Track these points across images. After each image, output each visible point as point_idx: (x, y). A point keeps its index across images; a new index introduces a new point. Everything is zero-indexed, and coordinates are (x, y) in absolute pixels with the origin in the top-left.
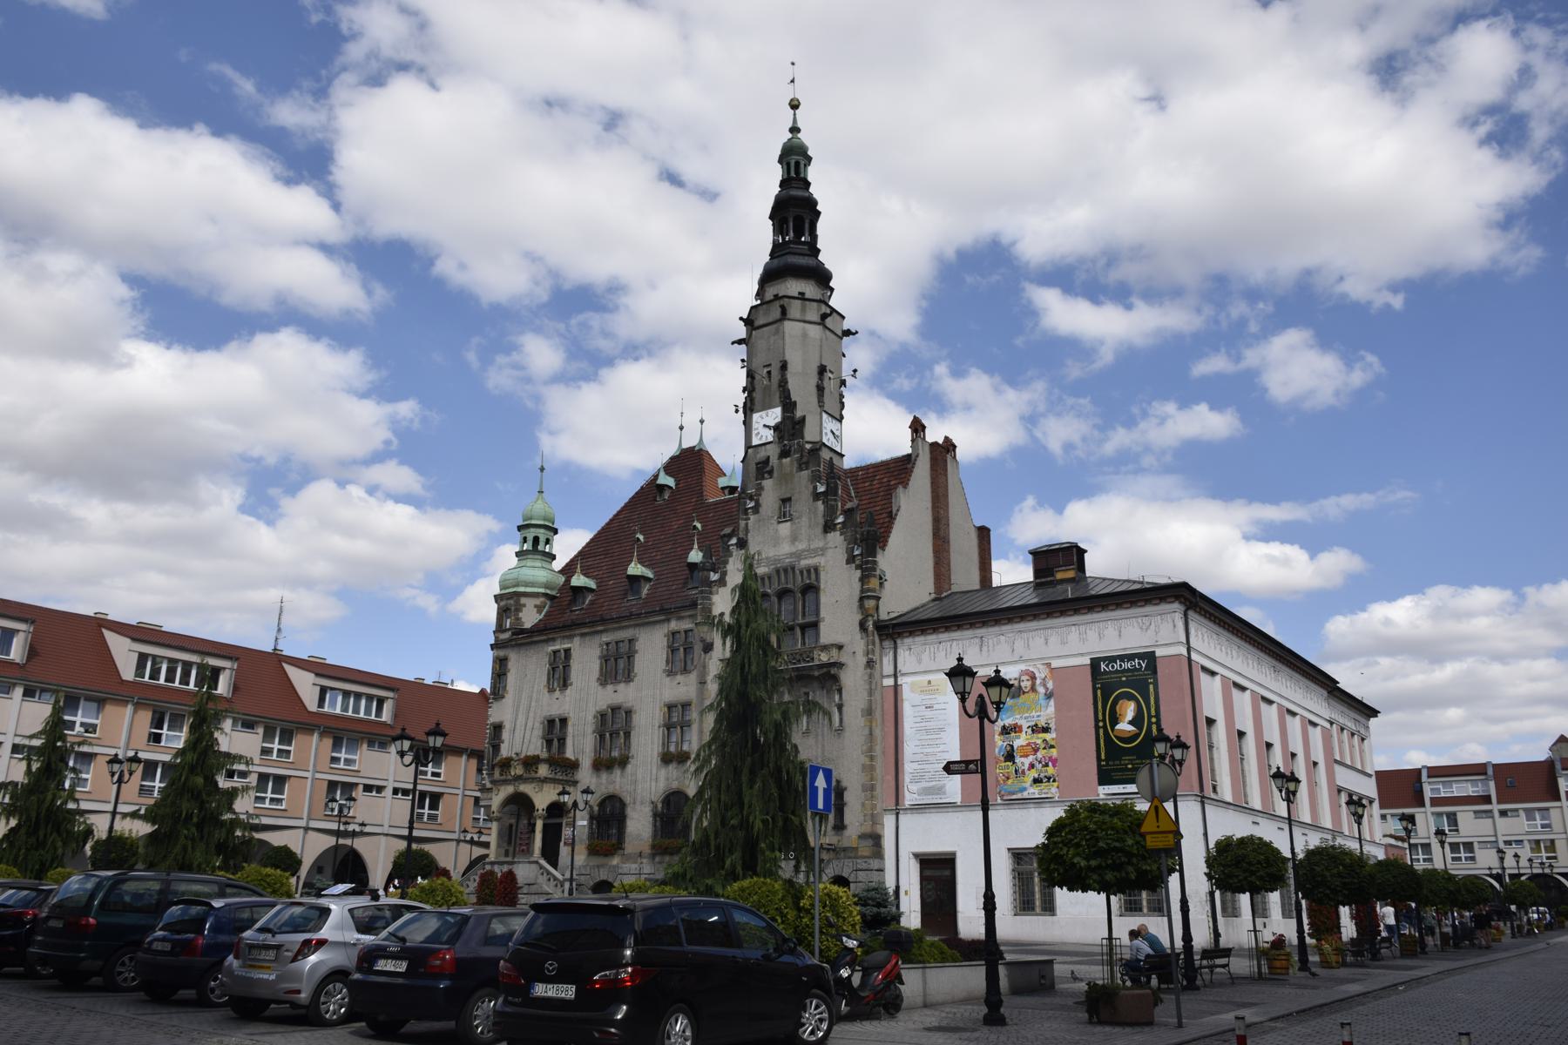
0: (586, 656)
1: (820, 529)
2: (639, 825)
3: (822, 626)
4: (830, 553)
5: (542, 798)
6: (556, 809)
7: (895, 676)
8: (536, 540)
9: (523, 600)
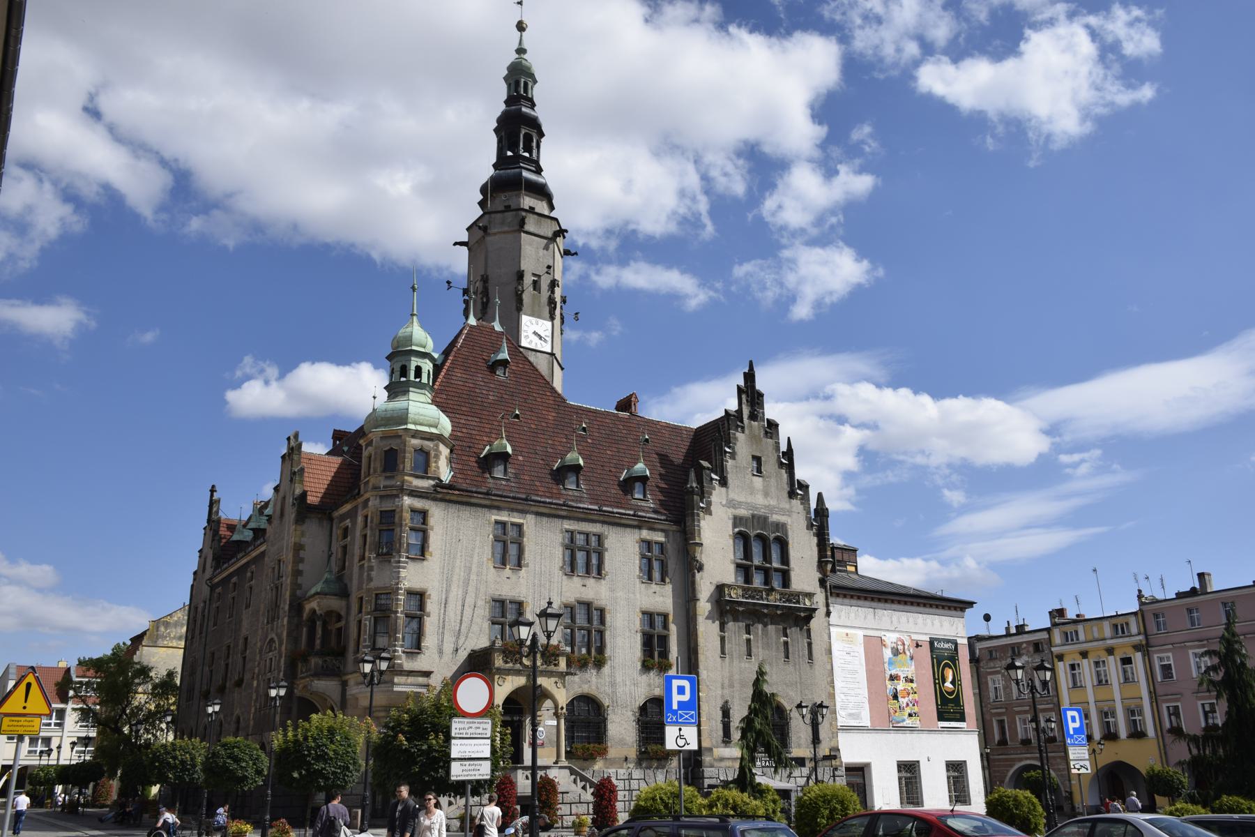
2: (622, 729)
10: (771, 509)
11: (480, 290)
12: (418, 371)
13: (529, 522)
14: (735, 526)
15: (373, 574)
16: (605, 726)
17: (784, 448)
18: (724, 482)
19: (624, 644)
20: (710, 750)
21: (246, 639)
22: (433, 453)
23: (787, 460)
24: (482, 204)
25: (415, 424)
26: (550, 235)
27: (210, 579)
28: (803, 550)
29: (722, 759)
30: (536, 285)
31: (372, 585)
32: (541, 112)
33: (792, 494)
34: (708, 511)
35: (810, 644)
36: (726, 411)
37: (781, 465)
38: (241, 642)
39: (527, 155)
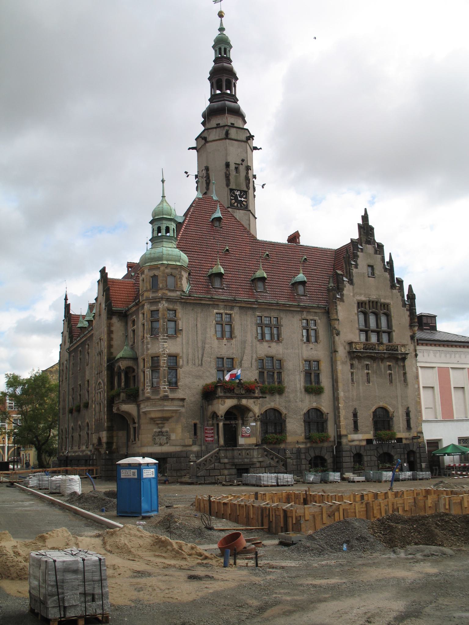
11: (205, 175)
12: (167, 230)
13: (236, 313)
14: (358, 307)
15: (149, 346)
16: (285, 424)
17: (387, 259)
18: (351, 282)
19: (294, 381)
20: (346, 436)
21: (88, 381)
22: (178, 276)
23: (390, 268)
24: (203, 124)
25: (167, 261)
26: (244, 139)
27: (69, 349)
28: (400, 318)
30: (236, 169)
31: (149, 352)
32: (236, 66)
33: (393, 286)
34: (342, 300)
35: (405, 374)
36: (351, 239)
37: (386, 270)
38: (86, 383)
39: (228, 92)
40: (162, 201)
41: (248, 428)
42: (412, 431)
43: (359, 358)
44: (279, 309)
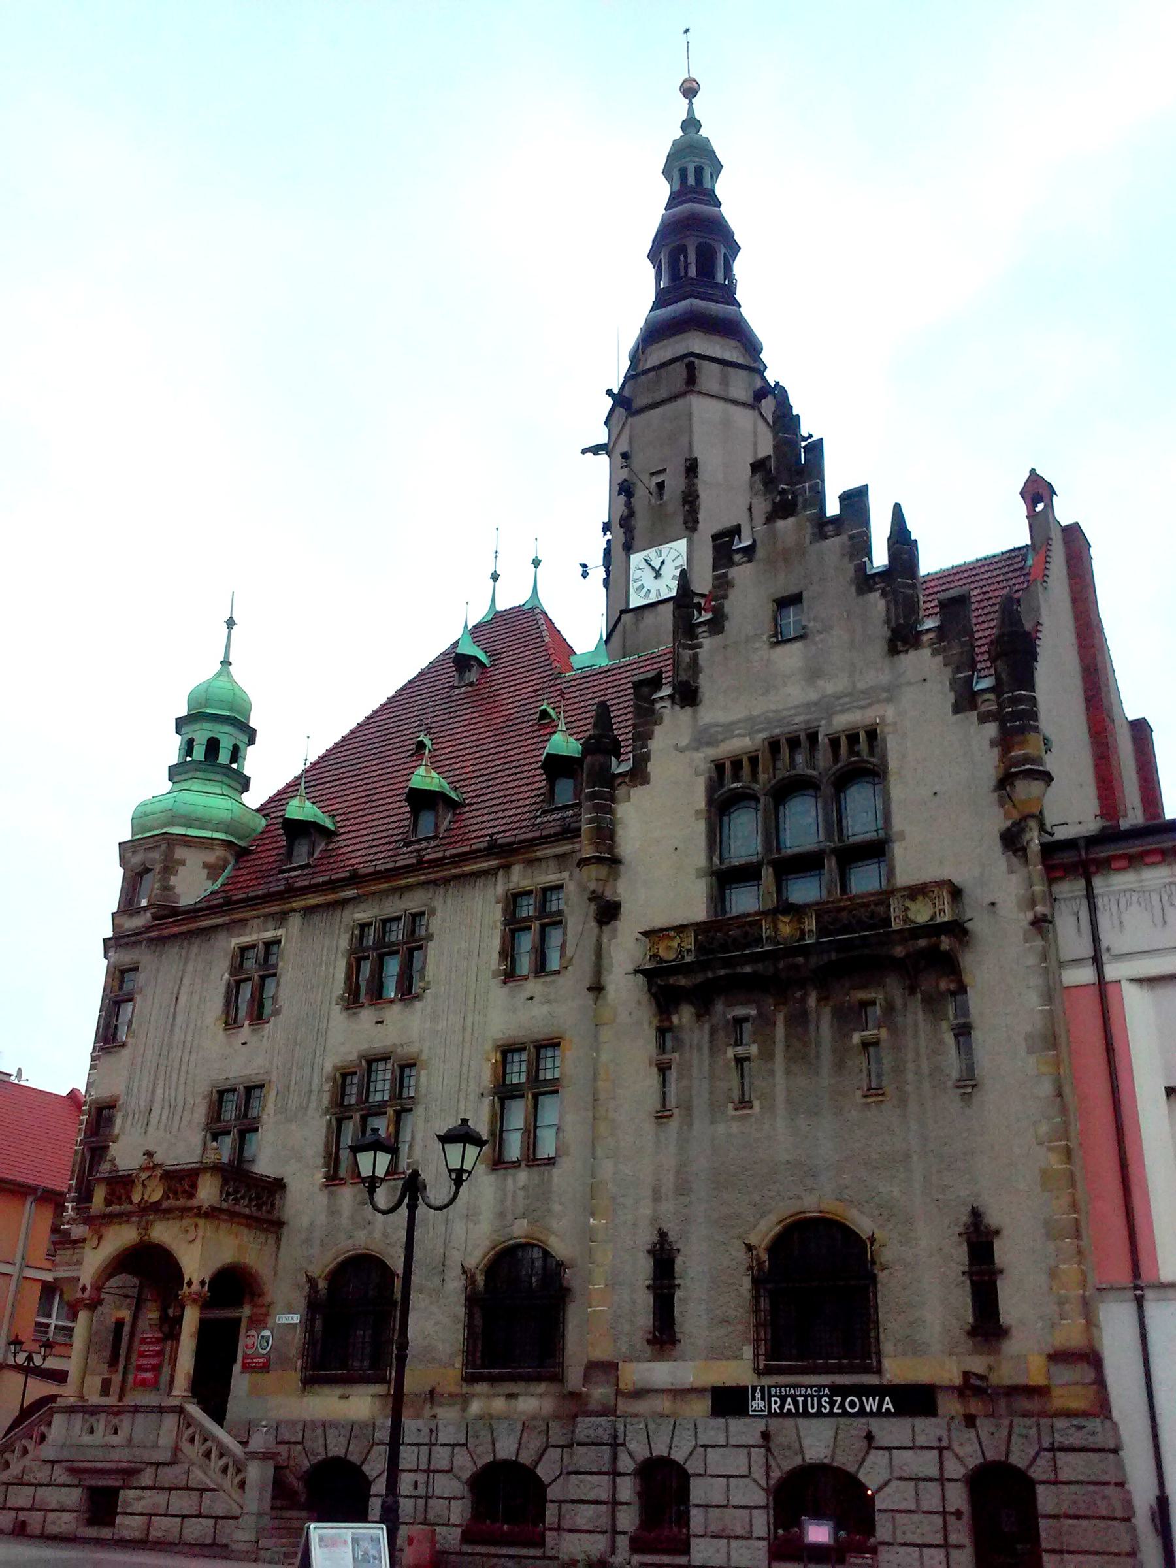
0: (313, 958)
1: (880, 646)
2: (435, 1325)
3: (898, 851)
4: (909, 697)
5: (197, 1256)
6: (234, 1286)
7: (1097, 961)
8: (213, 746)
9: (180, 853)
10: (827, 706)
20: (609, 1368)
29: (639, 1393)
40: (219, 674)
41: (266, 1333)
42: (1012, 1347)
43: (703, 1000)
44: (428, 883)
